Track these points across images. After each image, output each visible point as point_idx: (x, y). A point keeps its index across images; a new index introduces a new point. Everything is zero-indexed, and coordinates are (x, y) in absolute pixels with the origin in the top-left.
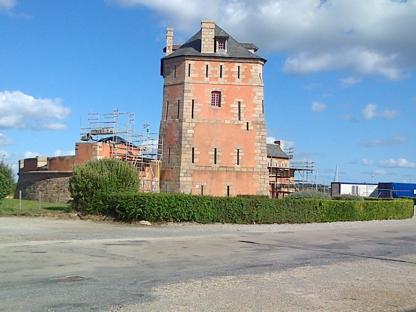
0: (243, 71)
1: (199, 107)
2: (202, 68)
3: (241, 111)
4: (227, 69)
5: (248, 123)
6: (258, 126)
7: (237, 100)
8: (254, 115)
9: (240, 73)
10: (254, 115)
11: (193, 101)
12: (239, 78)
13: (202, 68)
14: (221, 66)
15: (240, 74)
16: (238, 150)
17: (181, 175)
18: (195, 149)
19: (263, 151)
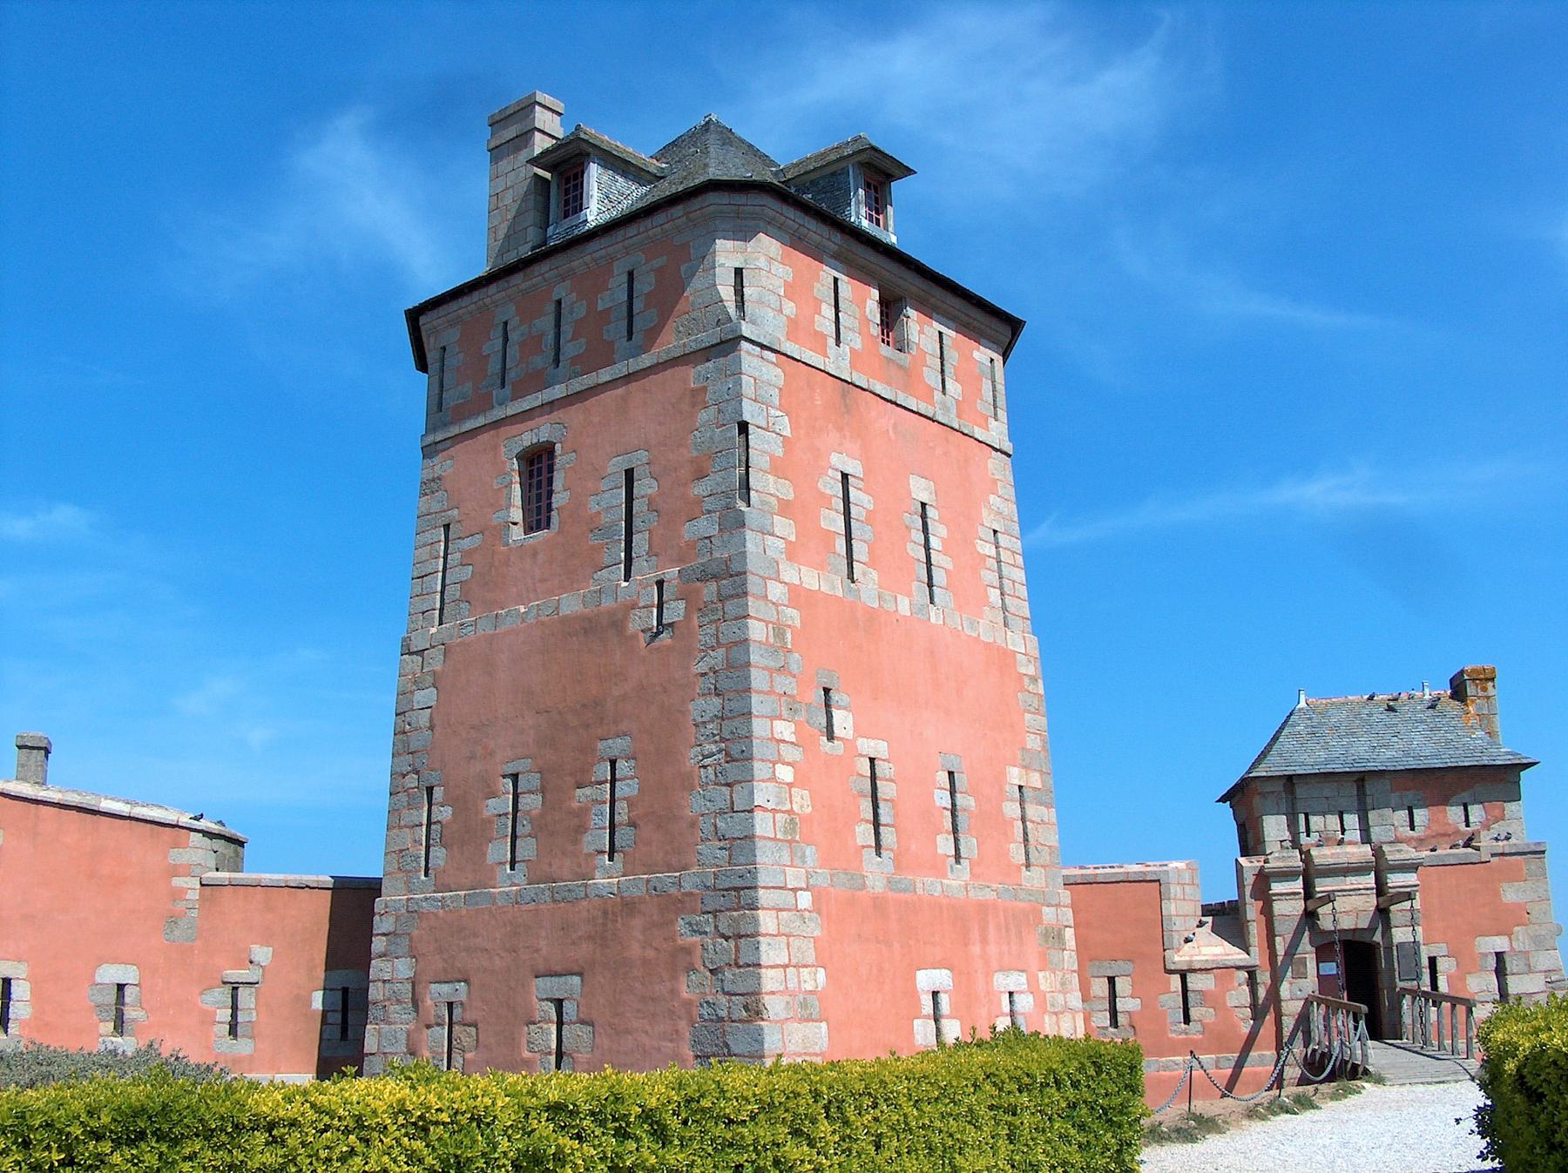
0: (647, 289)
1: (467, 554)
2: (486, 349)
3: (637, 522)
4: (581, 311)
5: (660, 584)
6: (709, 590)
7: (617, 466)
8: (691, 531)
9: (638, 306)
10: (691, 531)
11: (447, 527)
12: (630, 338)
13: (486, 350)
14: (559, 302)
15: (636, 311)
16: (613, 763)
17: (378, 944)
18: (438, 793)
19: (735, 750)
